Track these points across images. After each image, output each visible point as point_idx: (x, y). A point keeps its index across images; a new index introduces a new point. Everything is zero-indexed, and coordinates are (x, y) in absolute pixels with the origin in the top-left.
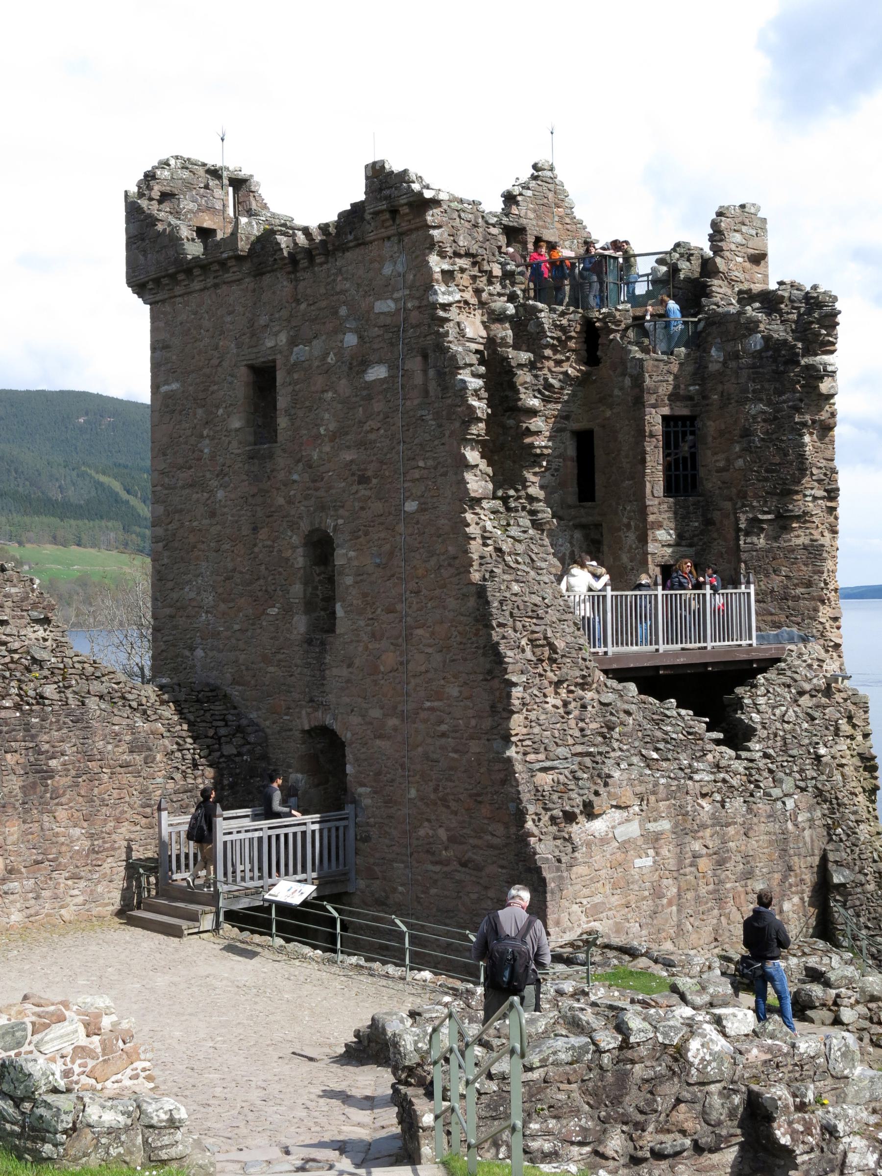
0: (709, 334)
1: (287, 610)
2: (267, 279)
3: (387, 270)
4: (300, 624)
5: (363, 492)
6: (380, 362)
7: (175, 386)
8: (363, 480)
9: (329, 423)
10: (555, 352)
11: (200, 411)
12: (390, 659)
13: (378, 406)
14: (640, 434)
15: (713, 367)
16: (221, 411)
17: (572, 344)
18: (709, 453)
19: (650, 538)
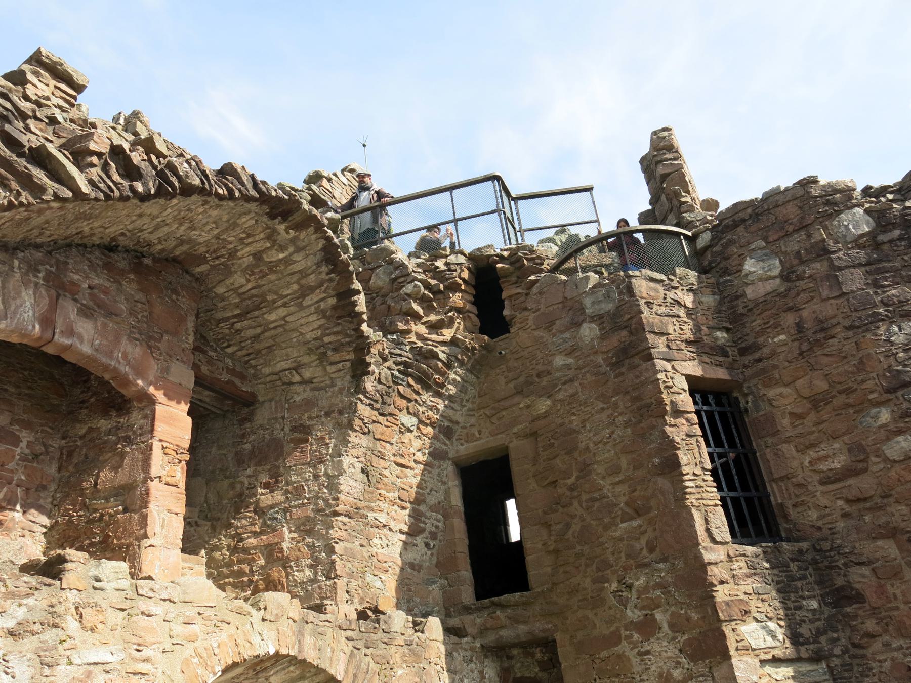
0: (731, 242)
10: (429, 309)
14: (651, 409)
17: (457, 299)
18: (789, 450)
19: (732, 644)
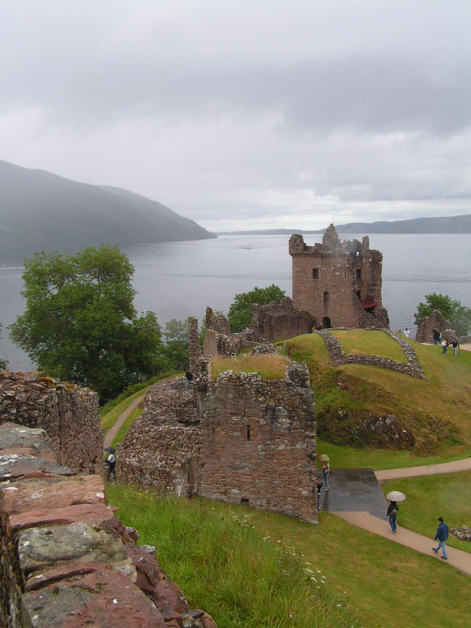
1: (320, 302)
2: (317, 258)
3: (339, 261)
4: (323, 303)
5: (335, 288)
7: (297, 269)
8: (335, 286)
9: (328, 278)
12: (339, 309)
15: (364, 262)
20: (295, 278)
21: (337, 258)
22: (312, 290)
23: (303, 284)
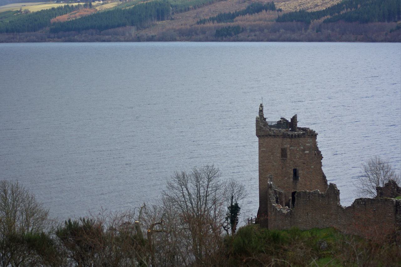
1: (289, 178)
4: (292, 180)
5: (304, 165)
6: (308, 151)
7: (264, 149)
8: (304, 164)
9: (298, 156)
11: (270, 153)
13: (307, 155)
16: (275, 153)
20: (262, 158)
21: (306, 138)
22: (281, 168)
23: (271, 163)
